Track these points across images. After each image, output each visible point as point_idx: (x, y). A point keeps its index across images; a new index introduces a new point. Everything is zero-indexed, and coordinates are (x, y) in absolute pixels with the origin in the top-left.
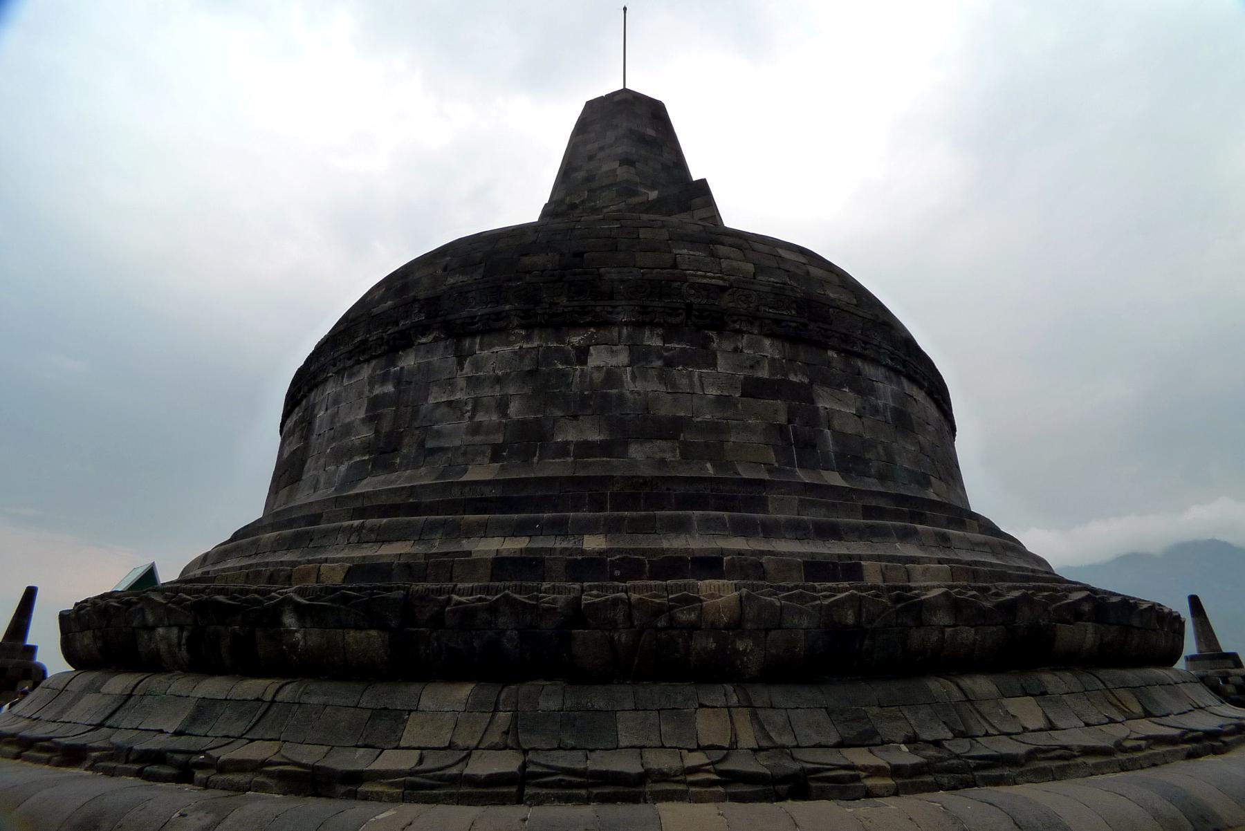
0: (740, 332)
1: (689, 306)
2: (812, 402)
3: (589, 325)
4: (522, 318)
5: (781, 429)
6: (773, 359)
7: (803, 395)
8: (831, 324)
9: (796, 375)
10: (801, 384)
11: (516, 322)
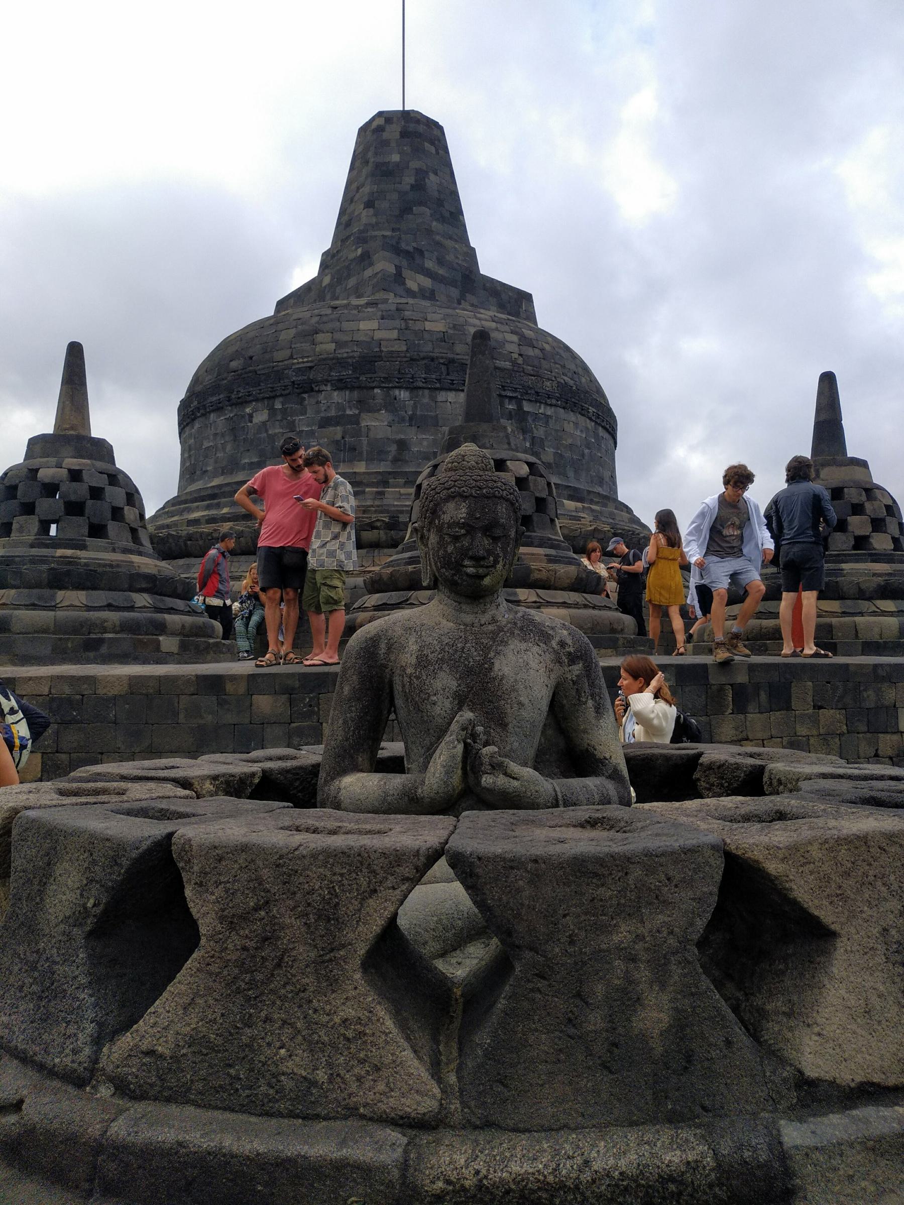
0: (319, 391)
1: (293, 382)
2: (358, 423)
3: (251, 401)
4: (229, 401)
5: (337, 442)
6: (338, 403)
7: (355, 420)
8: (375, 373)
9: (351, 410)
10: (354, 415)
11: (227, 403)
